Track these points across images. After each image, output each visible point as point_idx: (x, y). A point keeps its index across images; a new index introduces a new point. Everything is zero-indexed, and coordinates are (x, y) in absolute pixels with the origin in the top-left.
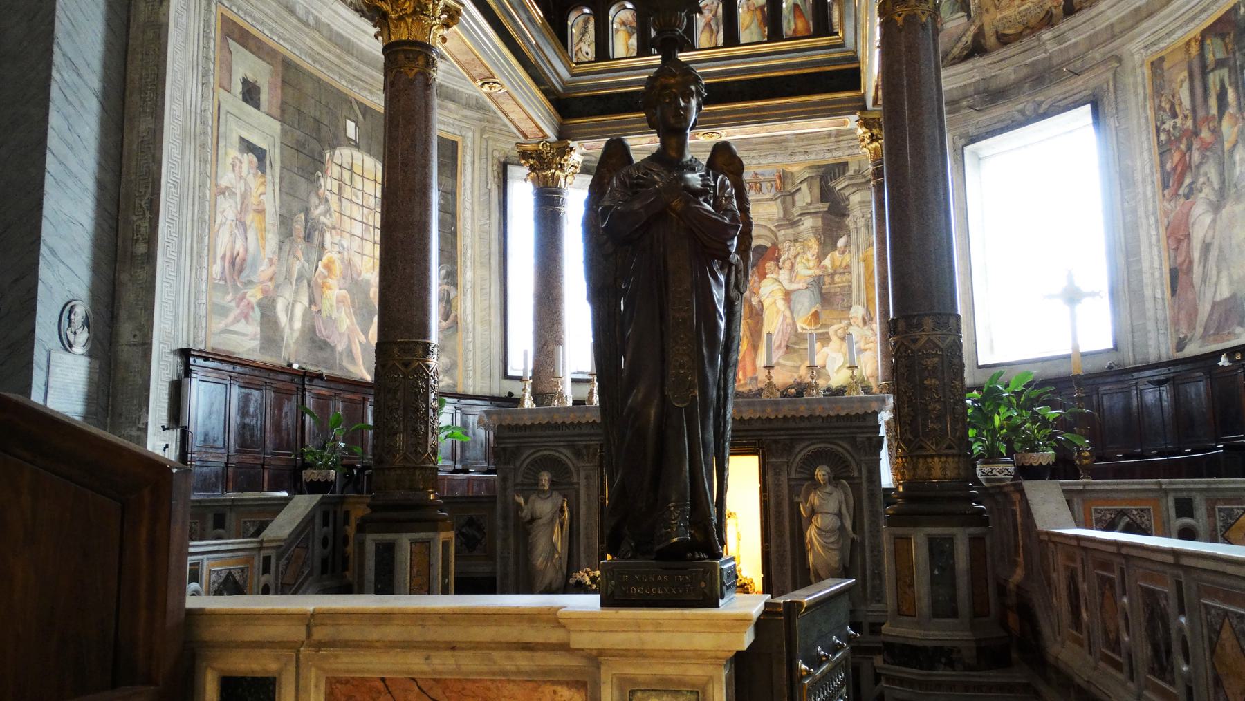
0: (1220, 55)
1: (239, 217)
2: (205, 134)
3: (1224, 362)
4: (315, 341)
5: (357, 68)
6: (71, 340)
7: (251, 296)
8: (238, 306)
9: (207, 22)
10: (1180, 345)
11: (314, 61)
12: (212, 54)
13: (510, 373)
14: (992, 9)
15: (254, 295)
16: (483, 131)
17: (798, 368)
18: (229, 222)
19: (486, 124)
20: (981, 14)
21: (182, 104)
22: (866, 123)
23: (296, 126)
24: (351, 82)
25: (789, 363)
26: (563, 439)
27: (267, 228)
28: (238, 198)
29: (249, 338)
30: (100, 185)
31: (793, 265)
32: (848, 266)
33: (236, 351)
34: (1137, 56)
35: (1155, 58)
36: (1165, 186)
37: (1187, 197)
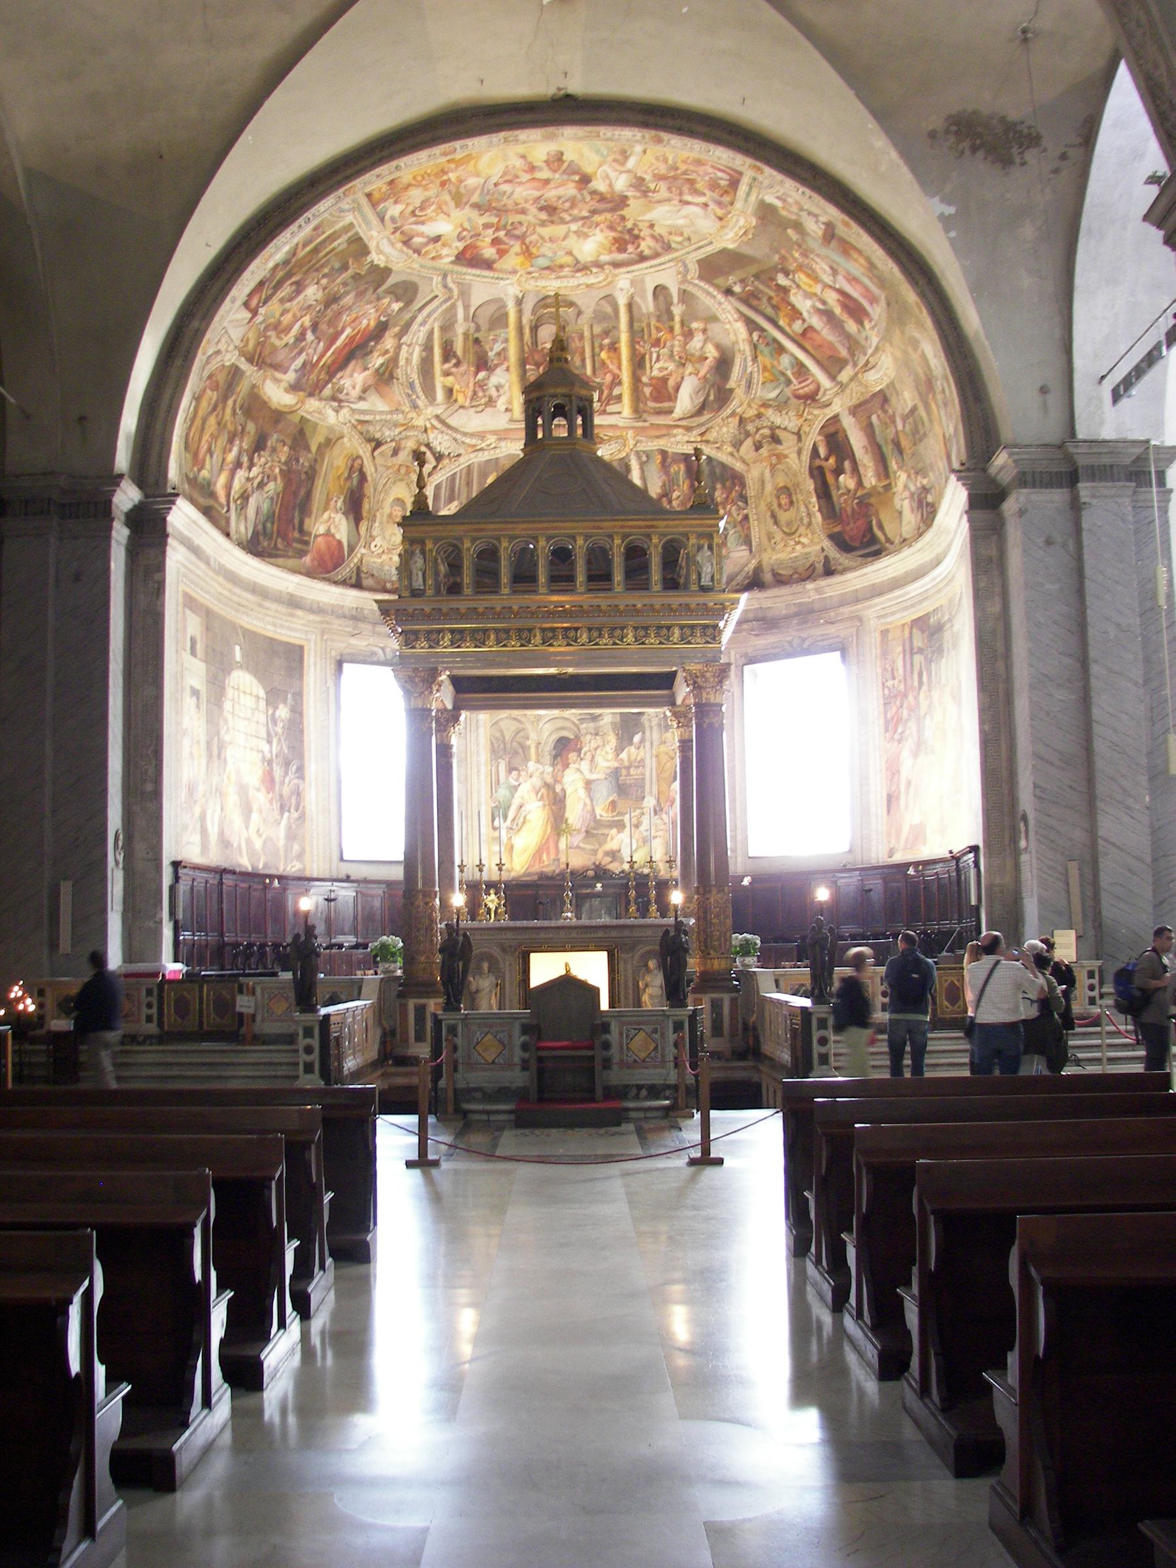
0: (920, 645)
3: (911, 871)
4: (225, 843)
5: (239, 596)
10: (891, 854)
11: (220, 601)
13: (345, 858)
14: (769, 550)
15: (197, 811)
16: (323, 633)
17: (595, 852)
19: (325, 626)
20: (760, 552)
22: (675, 714)
24: (237, 610)
25: (588, 847)
31: (593, 757)
32: (642, 760)
34: (872, 622)
35: (884, 628)
36: (887, 730)
37: (899, 742)
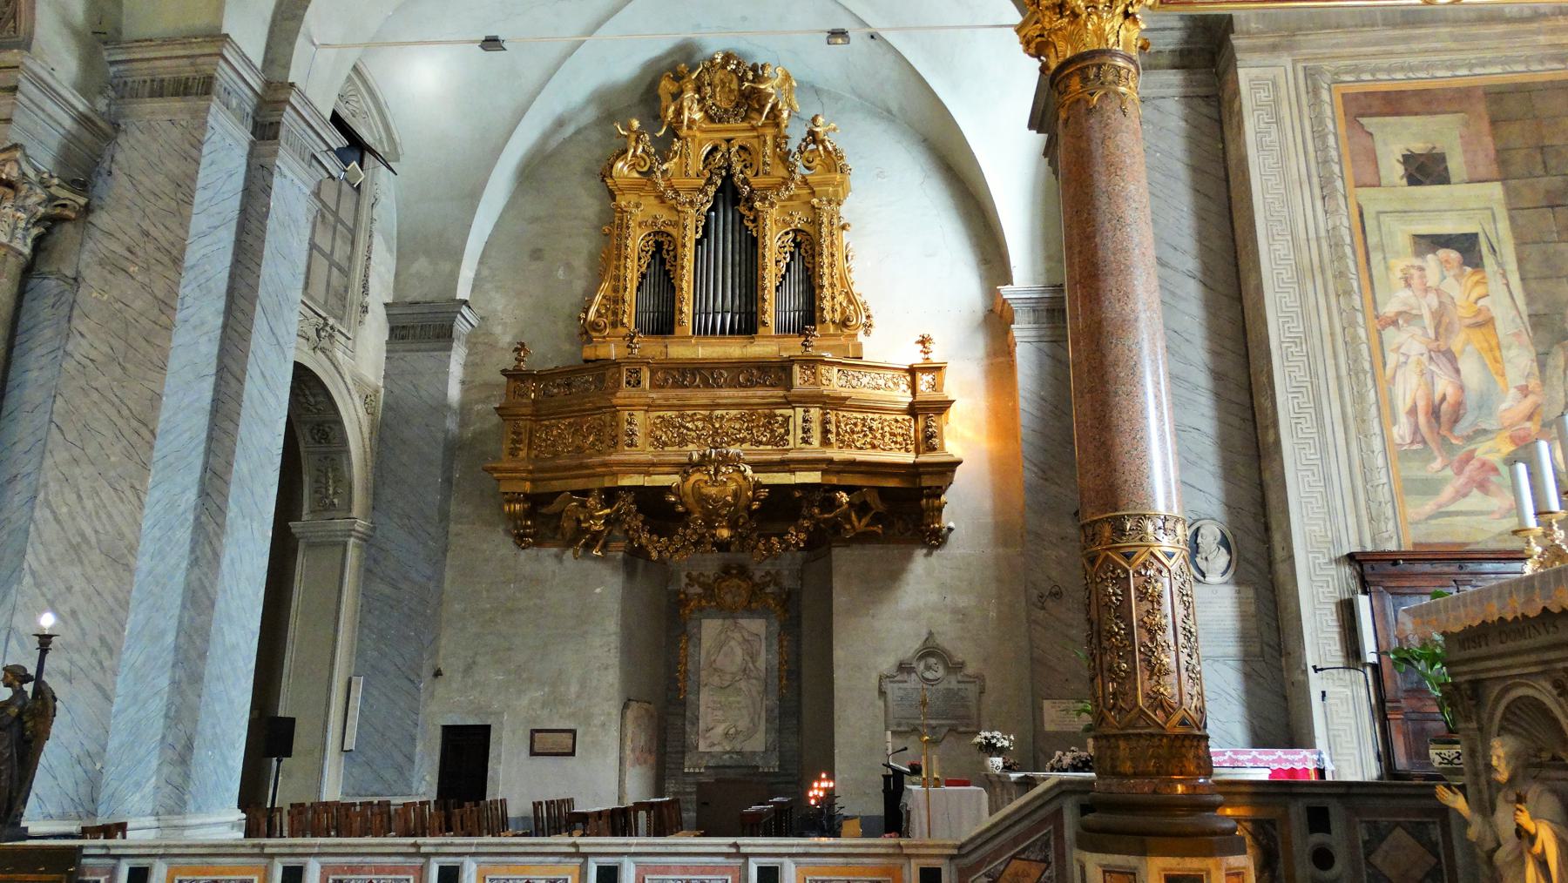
1: (1434, 345)
2: (1342, 257)
6: (1203, 569)
7: (1486, 453)
8: (1459, 472)
9: (1318, 120)
12: (1334, 154)
18: (1413, 359)
21: (1289, 238)
23: (1539, 169)
26: (1533, 657)
27: (1504, 341)
28: (1428, 320)
29: (1497, 516)
30: (1218, 376)
33: (1471, 540)
